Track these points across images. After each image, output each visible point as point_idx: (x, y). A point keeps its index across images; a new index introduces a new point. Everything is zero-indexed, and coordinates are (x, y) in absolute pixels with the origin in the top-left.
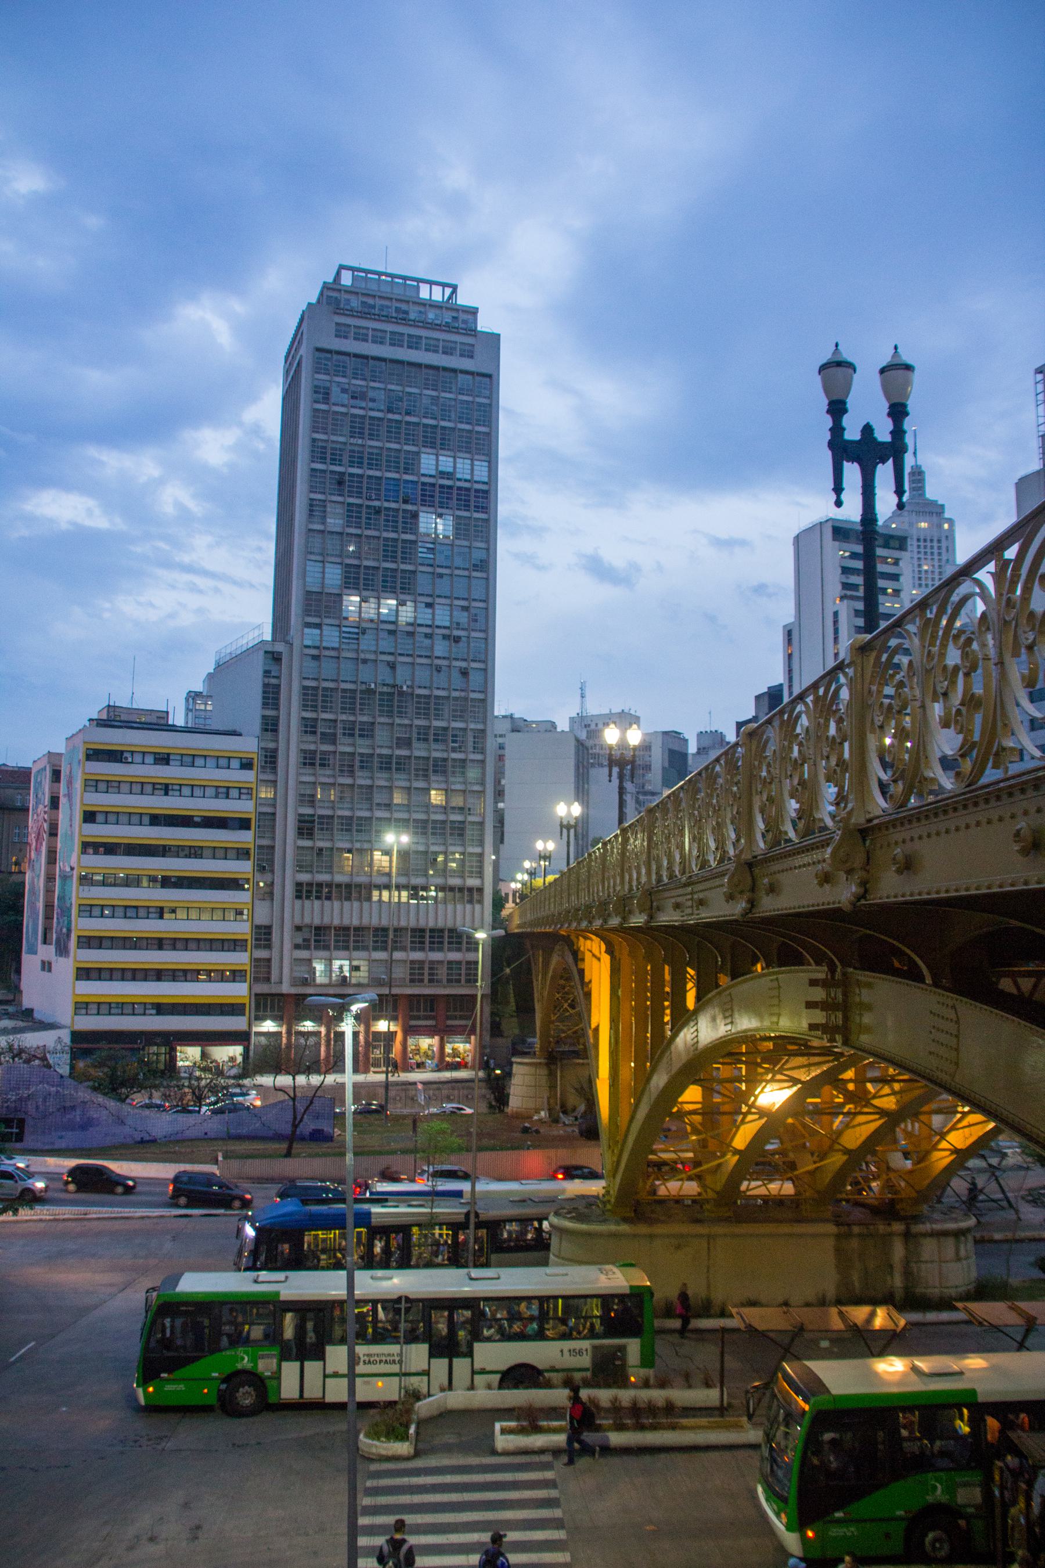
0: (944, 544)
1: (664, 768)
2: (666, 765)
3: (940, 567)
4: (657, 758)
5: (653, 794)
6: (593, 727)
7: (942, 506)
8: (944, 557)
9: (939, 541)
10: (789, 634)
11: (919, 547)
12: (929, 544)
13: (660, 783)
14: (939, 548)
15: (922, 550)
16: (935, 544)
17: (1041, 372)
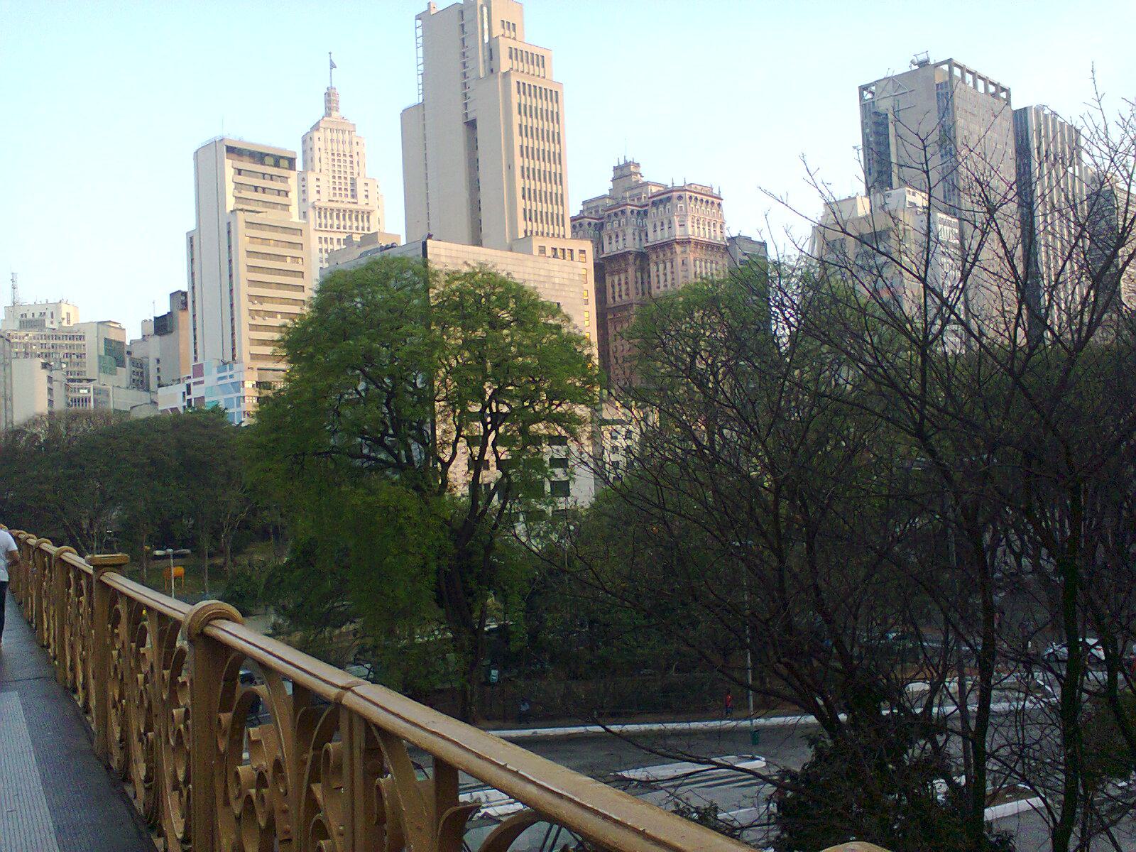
0: (355, 159)
1: (100, 356)
2: (103, 353)
3: (352, 179)
4: (93, 348)
5: (89, 381)
6: (29, 316)
7: (354, 125)
8: (356, 172)
9: (351, 156)
10: (191, 240)
11: (333, 160)
12: (342, 158)
13: (96, 369)
14: (352, 162)
15: (336, 163)
16: (348, 159)
17: (420, 19)
